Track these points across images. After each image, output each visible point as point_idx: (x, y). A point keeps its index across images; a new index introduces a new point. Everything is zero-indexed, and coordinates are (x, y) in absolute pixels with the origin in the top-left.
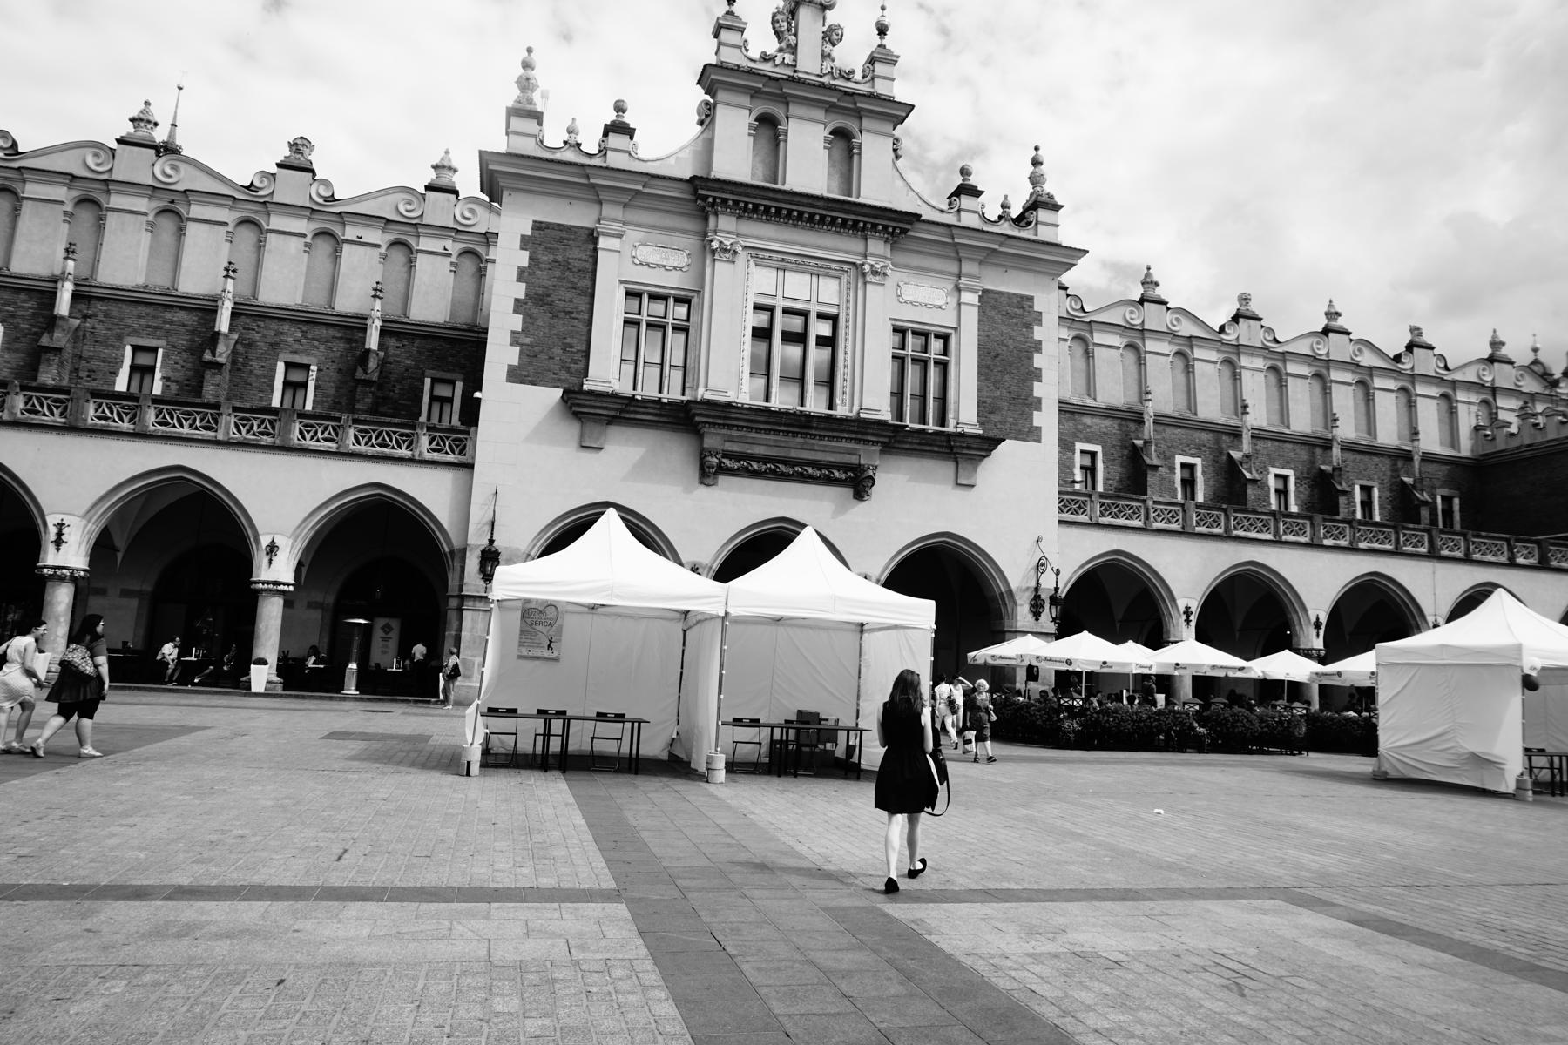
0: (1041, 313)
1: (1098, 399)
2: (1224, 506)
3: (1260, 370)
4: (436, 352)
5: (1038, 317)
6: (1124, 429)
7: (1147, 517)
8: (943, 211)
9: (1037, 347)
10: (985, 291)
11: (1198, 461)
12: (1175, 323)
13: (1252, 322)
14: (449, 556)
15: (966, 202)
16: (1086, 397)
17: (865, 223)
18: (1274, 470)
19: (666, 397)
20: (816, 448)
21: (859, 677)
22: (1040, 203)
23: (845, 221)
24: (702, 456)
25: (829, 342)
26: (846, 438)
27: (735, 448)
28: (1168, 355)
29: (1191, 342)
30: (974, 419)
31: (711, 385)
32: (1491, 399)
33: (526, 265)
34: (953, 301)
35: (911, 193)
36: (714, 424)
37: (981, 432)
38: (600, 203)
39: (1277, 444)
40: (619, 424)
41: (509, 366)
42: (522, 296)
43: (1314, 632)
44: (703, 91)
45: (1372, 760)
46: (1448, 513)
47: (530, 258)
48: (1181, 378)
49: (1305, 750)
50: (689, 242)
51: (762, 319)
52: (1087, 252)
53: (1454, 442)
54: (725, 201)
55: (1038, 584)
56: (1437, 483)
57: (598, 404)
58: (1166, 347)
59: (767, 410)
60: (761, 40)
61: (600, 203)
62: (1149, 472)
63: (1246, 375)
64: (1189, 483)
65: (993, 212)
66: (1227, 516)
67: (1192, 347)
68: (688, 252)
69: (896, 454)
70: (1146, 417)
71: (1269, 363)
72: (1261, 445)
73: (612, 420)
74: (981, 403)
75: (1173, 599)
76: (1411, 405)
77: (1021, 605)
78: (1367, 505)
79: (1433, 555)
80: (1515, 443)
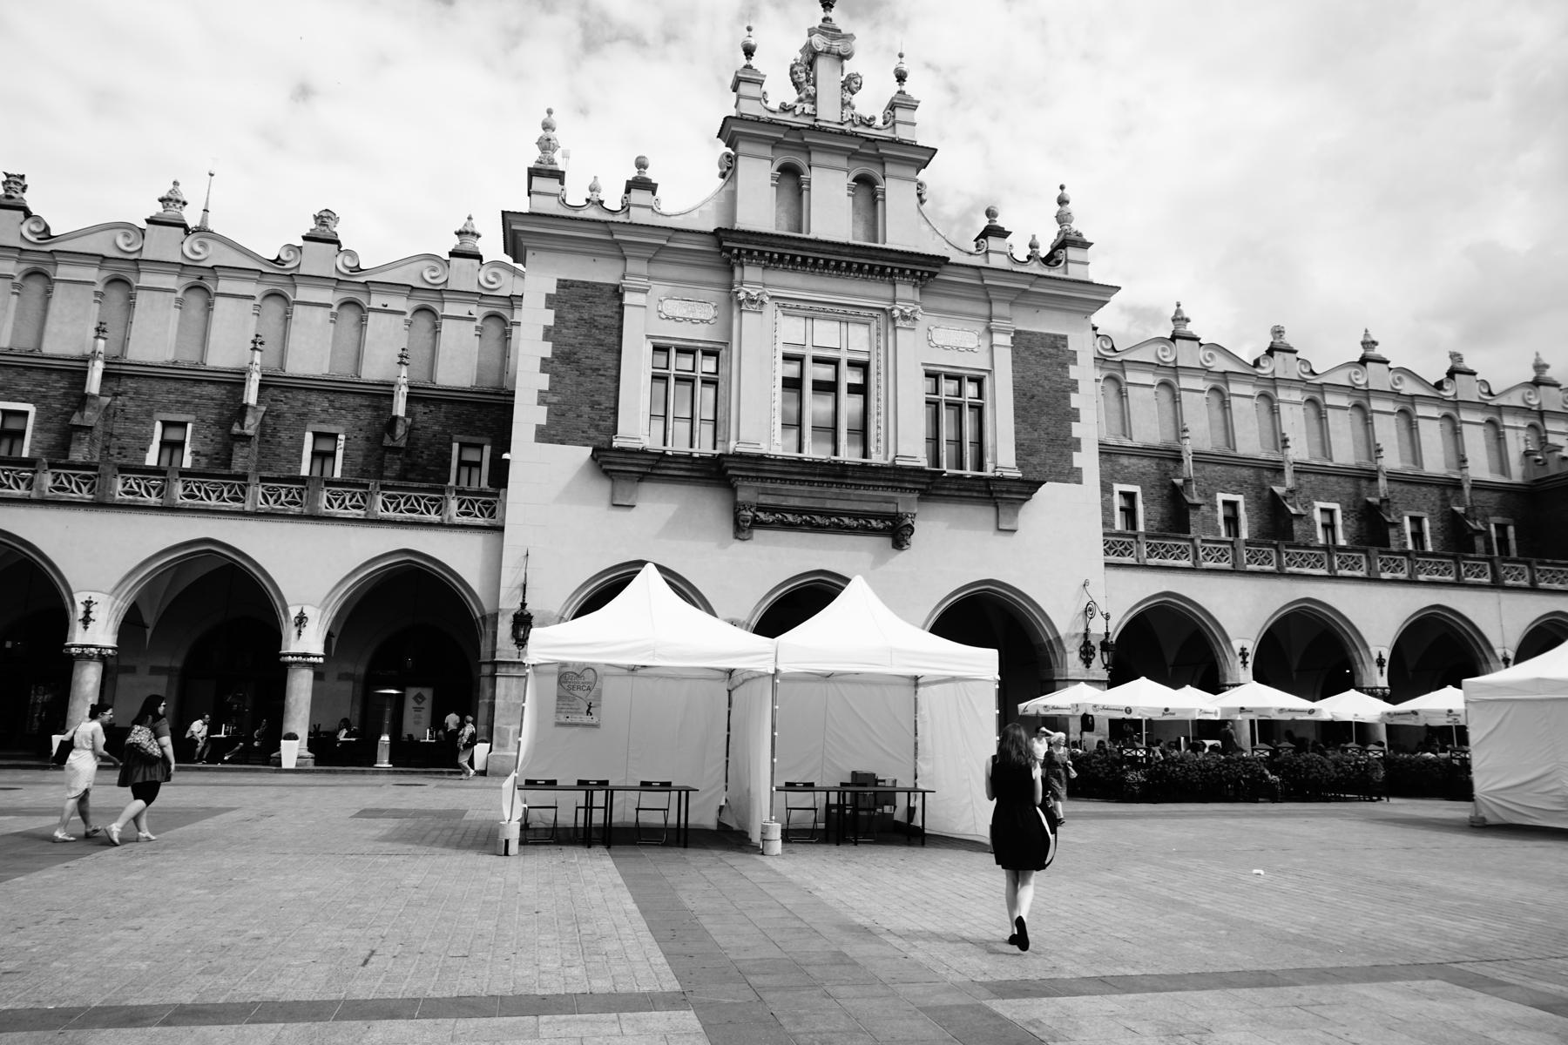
0: (1075, 352)
1: (1134, 439)
2: (1275, 542)
3: (1298, 403)
6: (1162, 468)
7: (1196, 557)
8: (970, 254)
9: (1074, 386)
10: (1017, 332)
11: (1240, 498)
12: (1209, 359)
13: (1287, 355)
14: (480, 622)
15: (993, 243)
16: (1122, 437)
17: (893, 268)
18: (1319, 505)
19: (697, 451)
20: (852, 497)
21: (916, 734)
22: (1068, 241)
23: (872, 267)
24: (736, 510)
25: (861, 390)
26: (883, 487)
27: (770, 500)
28: (1203, 392)
29: (1226, 377)
30: (1013, 463)
31: (742, 438)
32: (1538, 422)
33: (552, 324)
34: (985, 344)
35: (938, 237)
36: (748, 477)
37: (1020, 475)
38: (624, 259)
39: (1320, 477)
40: (651, 480)
41: (538, 426)
42: (548, 355)
43: (1377, 670)
44: (724, 144)
45: (1470, 805)
46: (1503, 541)
47: (556, 317)
48: (1218, 415)
49: (1384, 796)
50: (715, 294)
51: (792, 370)
52: (1119, 288)
53: (1503, 466)
54: (750, 252)
55: (1087, 629)
56: (1489, 511)
57: (629, 461)
58: (1201, 384)
59: (800, 461)
60: (779, 92)
61: (624, 259)
62: (1191, 511)
63: (1284, 409)
64: (1232, 521)
65: (1021, 253)
66: (1279, 553)
67: (1227, 383)
68: (714, 304)
69: (934, 501)
70: (1184, 455)
71: (1307, 396)
72: (1304, 479)
73: (643, 477)
74: (1018, 446)
75: (1227, 640)
76: (1456, 432)
77: (1071, 652)
78: (1418, 536)
79: (1497, 585)
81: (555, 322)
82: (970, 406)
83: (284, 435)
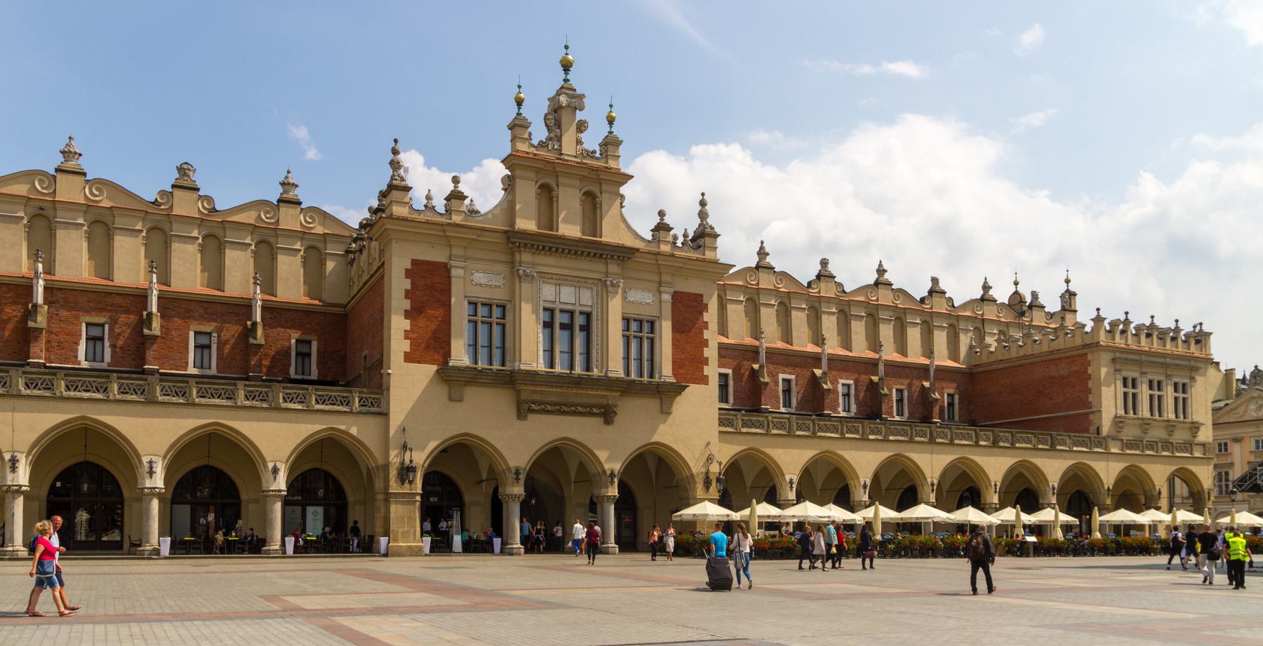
4: (297, 321)
5: (705, 307)
7: (768, 427)
14: (375, 469)
18: (842, 381)
25: (586, 328)
30: (670, 373)
32: (981, 326)
33: (410, 288)
37: (675, 381)
47: (412, 283)
54: (526, 245)
57: (461, 375)
64: (787, 392)
74: (674, 362)
80: (992, 359)
81: (412, 287)
82: (647, 338)
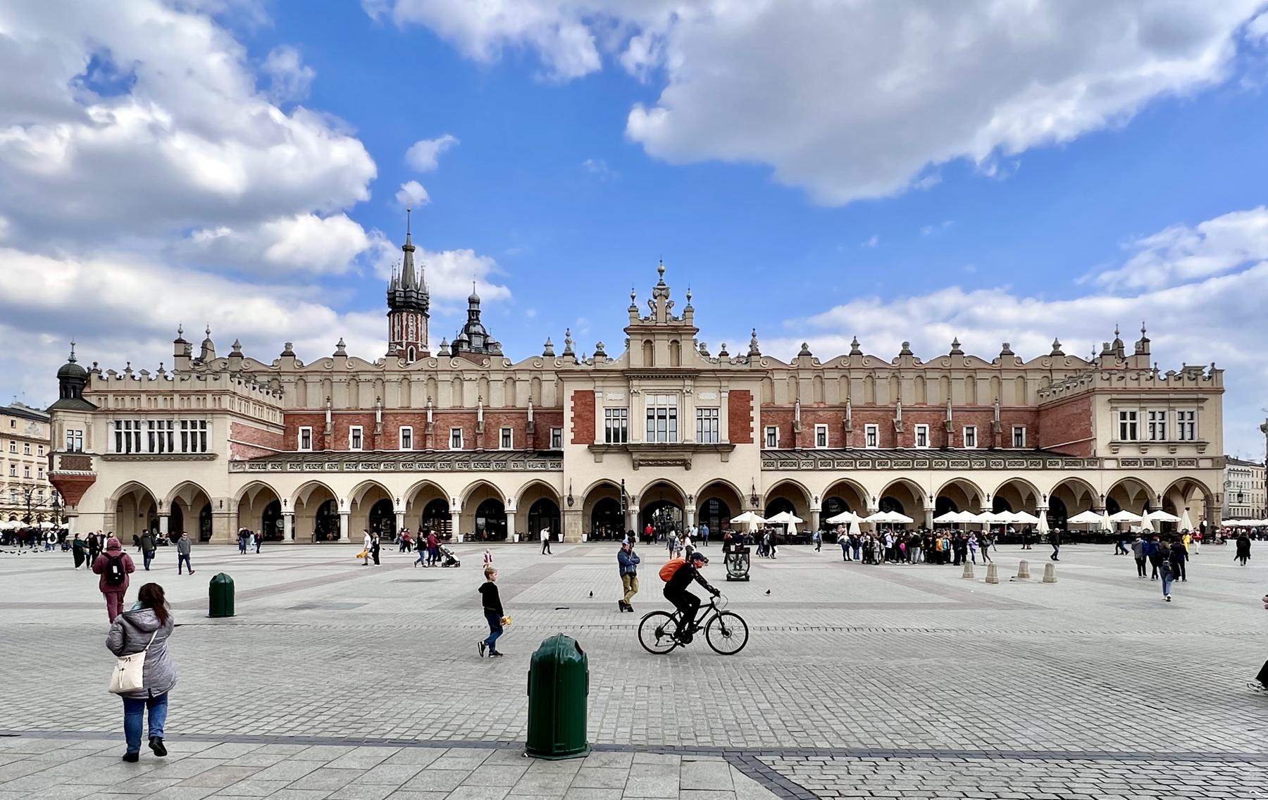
7: (799, 465)
24: (634, 461)
37: (728, 443)
38: (595, 381)
51: (651, 414)
61: (595, 381)
83: (492, 430)
